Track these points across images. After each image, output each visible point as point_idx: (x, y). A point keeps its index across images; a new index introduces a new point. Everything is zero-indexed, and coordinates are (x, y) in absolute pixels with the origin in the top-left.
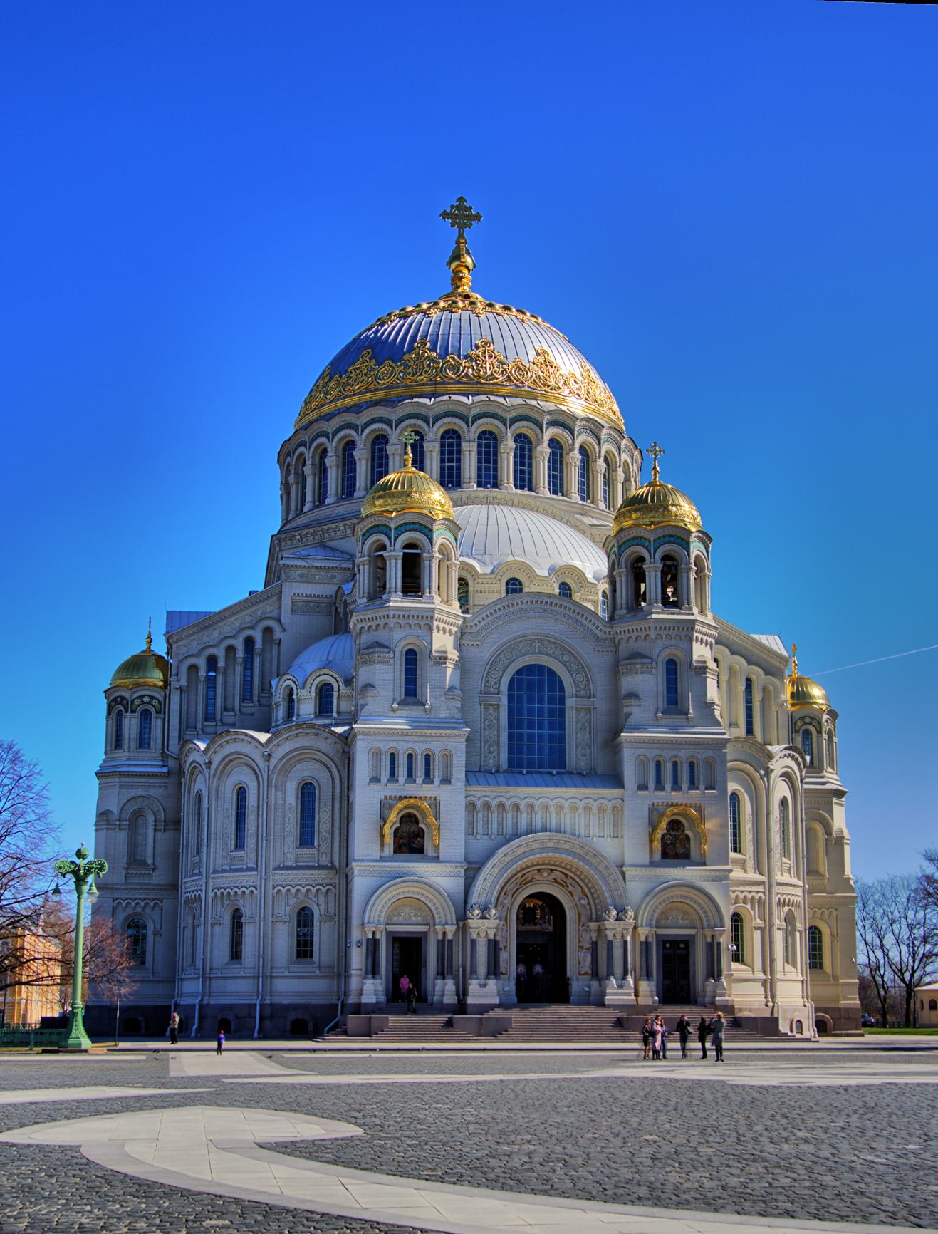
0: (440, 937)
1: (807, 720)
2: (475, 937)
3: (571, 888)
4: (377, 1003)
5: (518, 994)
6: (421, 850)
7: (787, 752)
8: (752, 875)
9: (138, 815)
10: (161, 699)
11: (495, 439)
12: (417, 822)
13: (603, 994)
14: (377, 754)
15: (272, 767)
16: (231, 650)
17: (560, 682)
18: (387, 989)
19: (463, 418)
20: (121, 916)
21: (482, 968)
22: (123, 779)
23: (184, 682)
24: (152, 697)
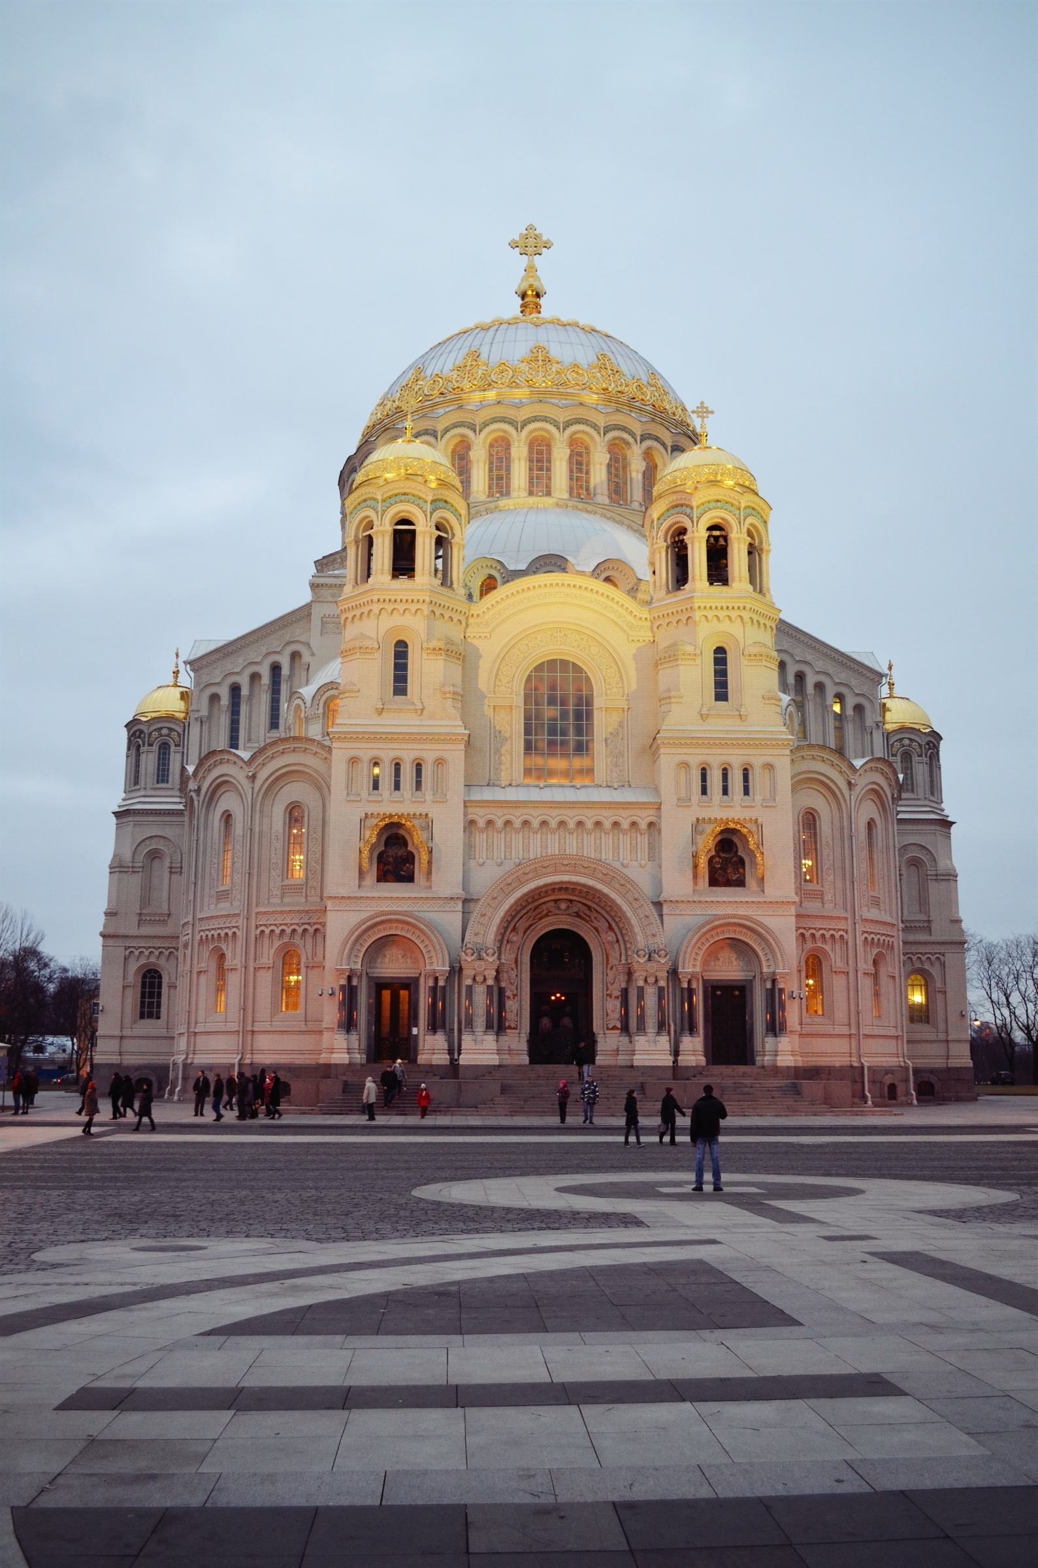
0: (431, 983)
1: (906, 742)
2: (469, 982)
3: (596, 924)
4: (350, 1064)
5: (531, 1053)
6: (410, 879)
7: (872, 765)
8: (829, 909)
9: (154, 855)
10: (181, 731)
11: (549, 446)
12: (405, 844)
13: (633, 1053)
14: (354, 761)
15: (256, 790)
16: (255, 677)
17: (588, 678)
18: (369, 1046)
19: (511, 422)
20: (133, 966)
21: (480, 1022)
22: (138, 818)
23: (204, 712)
24: (170, 729)
